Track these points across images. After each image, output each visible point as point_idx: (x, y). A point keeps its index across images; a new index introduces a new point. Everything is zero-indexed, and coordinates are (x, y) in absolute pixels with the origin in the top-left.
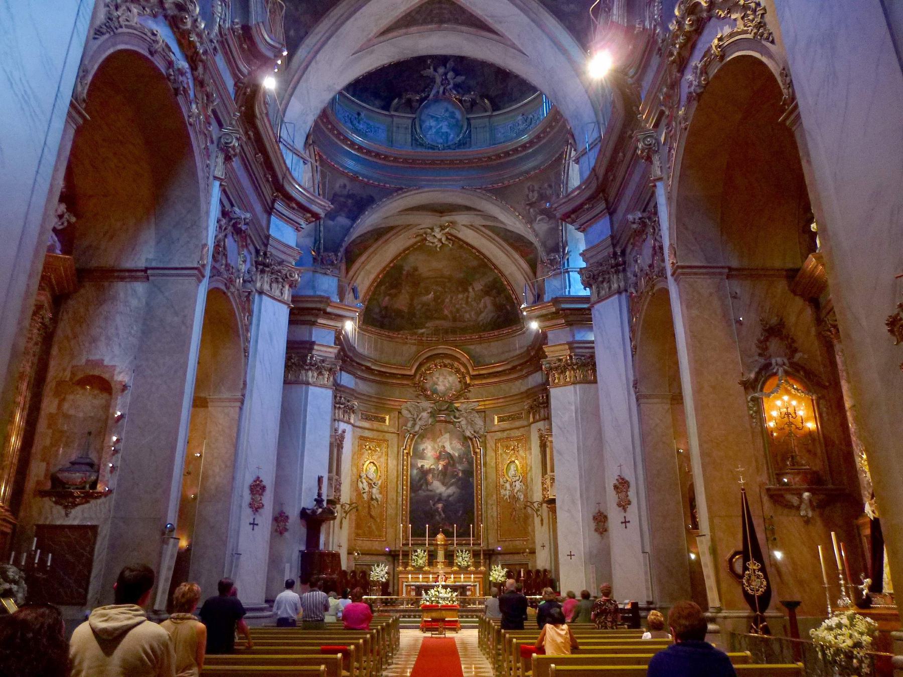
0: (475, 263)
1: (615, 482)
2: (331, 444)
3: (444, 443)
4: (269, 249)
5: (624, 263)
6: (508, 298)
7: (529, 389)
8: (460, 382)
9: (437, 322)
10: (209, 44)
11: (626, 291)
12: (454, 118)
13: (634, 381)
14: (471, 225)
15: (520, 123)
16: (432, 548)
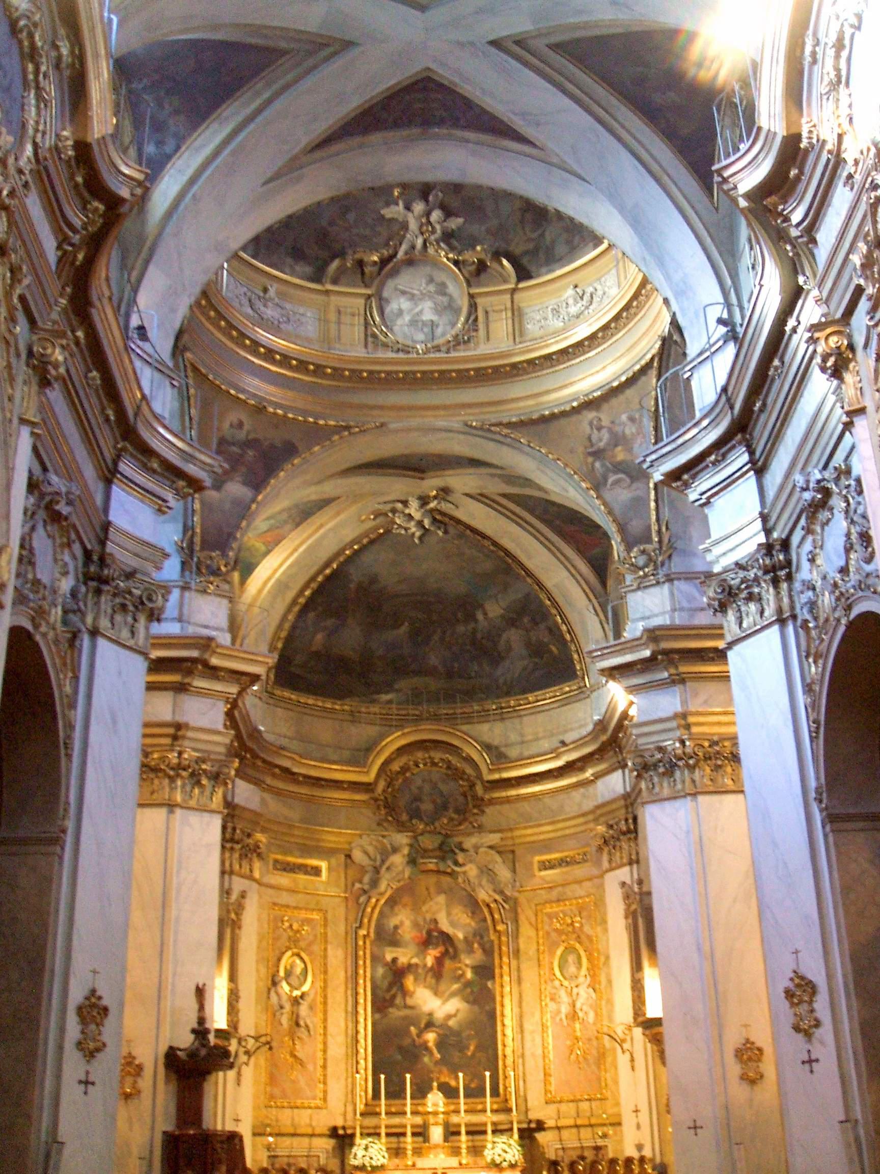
0: (488, 566)
1: (790, 985)
2: (222, 923)
3: (434, 914)
4: (108, 550)
5: (789, 563)
6: (554, 631)
7: (598, 807)
8: (465, 795)
9: (417, 681)
10: (17, 176)
11: (794, 617)
12: (444, 294)
13: (816, 788)
14: (482, 495)
15: (571, 301)
16: (418, 1120)
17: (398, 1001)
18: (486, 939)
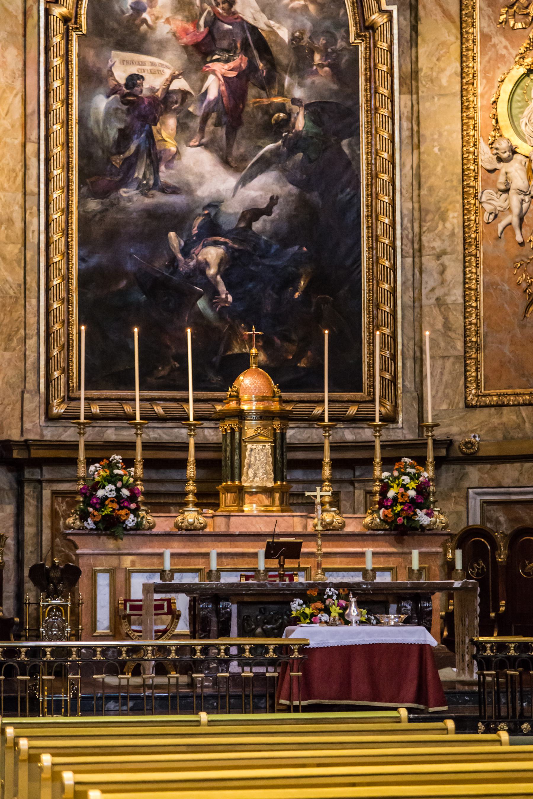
17: (139, 174)
18: (340, 44)
